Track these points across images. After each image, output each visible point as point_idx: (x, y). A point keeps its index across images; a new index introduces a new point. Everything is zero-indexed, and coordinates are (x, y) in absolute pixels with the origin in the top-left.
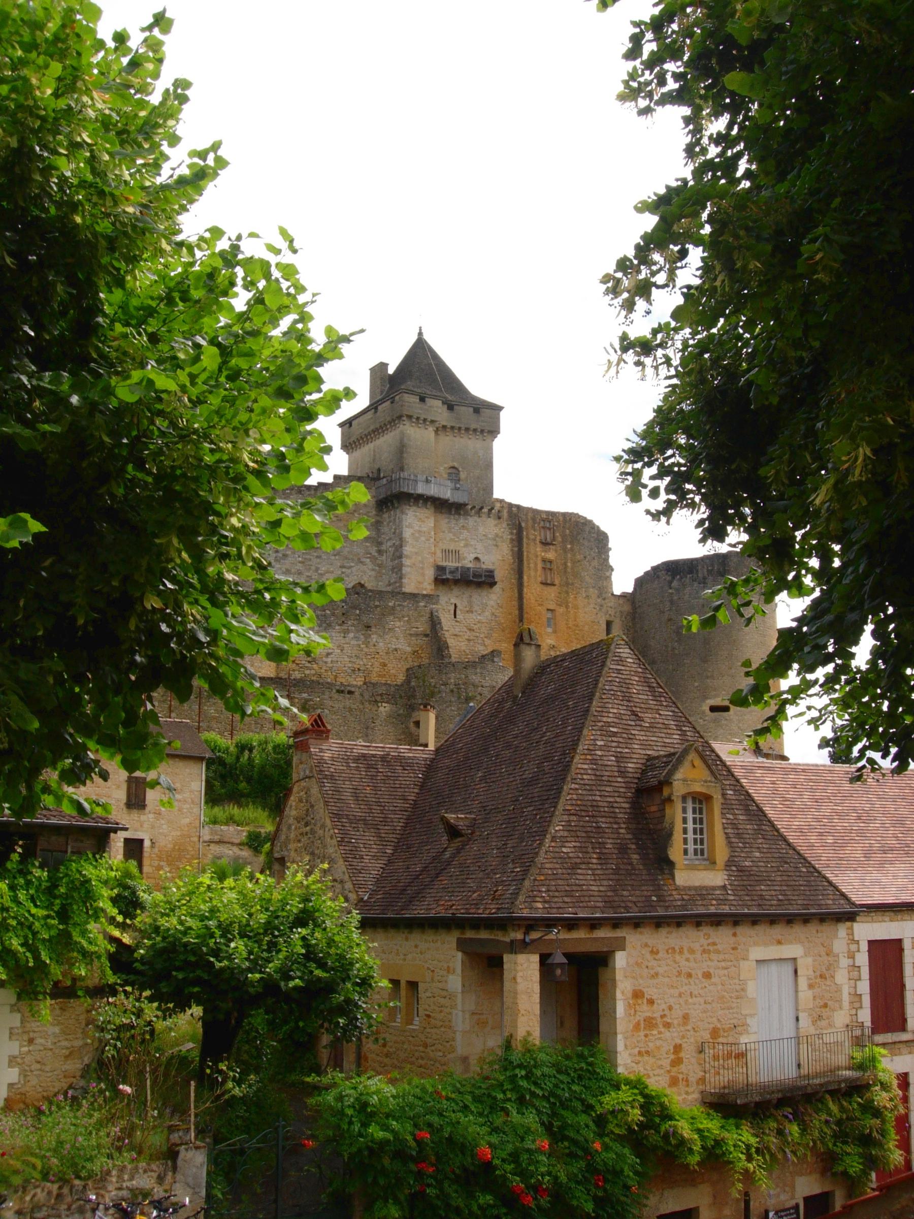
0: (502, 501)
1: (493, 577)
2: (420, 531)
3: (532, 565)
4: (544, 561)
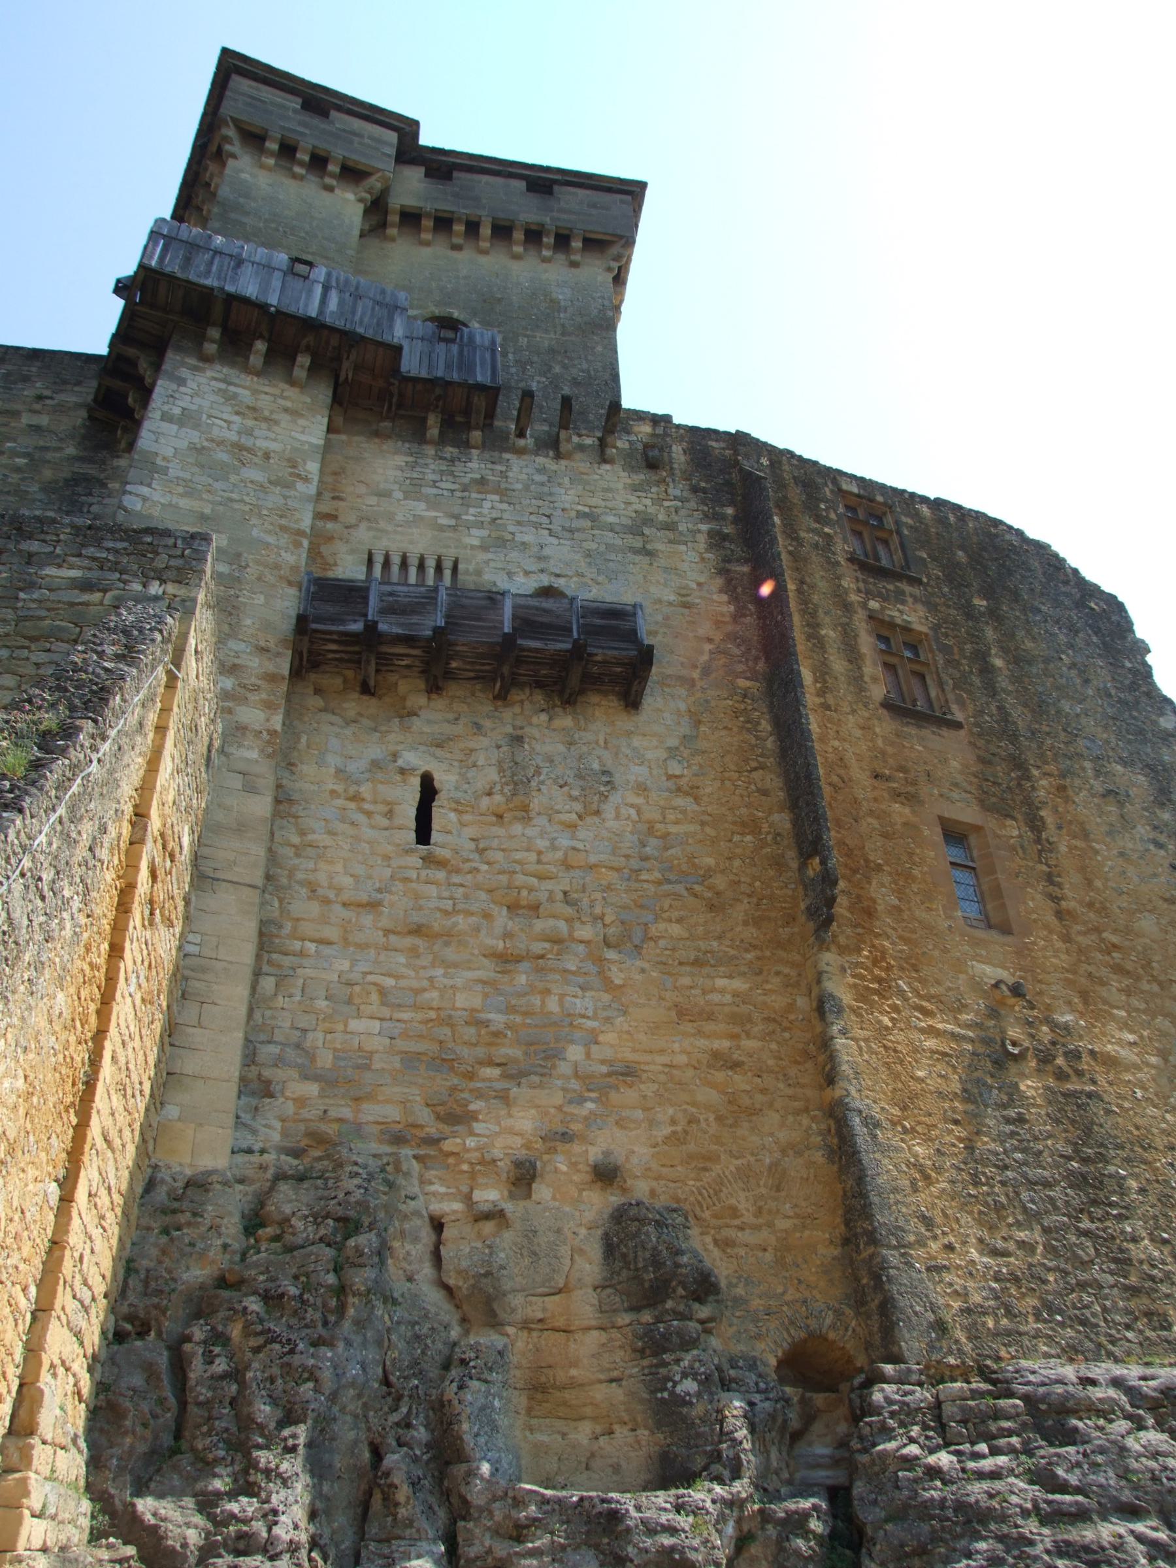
0: (661, 421)
1: (632, 635)
2: (241, 448)
3: (829, 633)
4: (884, 630)
